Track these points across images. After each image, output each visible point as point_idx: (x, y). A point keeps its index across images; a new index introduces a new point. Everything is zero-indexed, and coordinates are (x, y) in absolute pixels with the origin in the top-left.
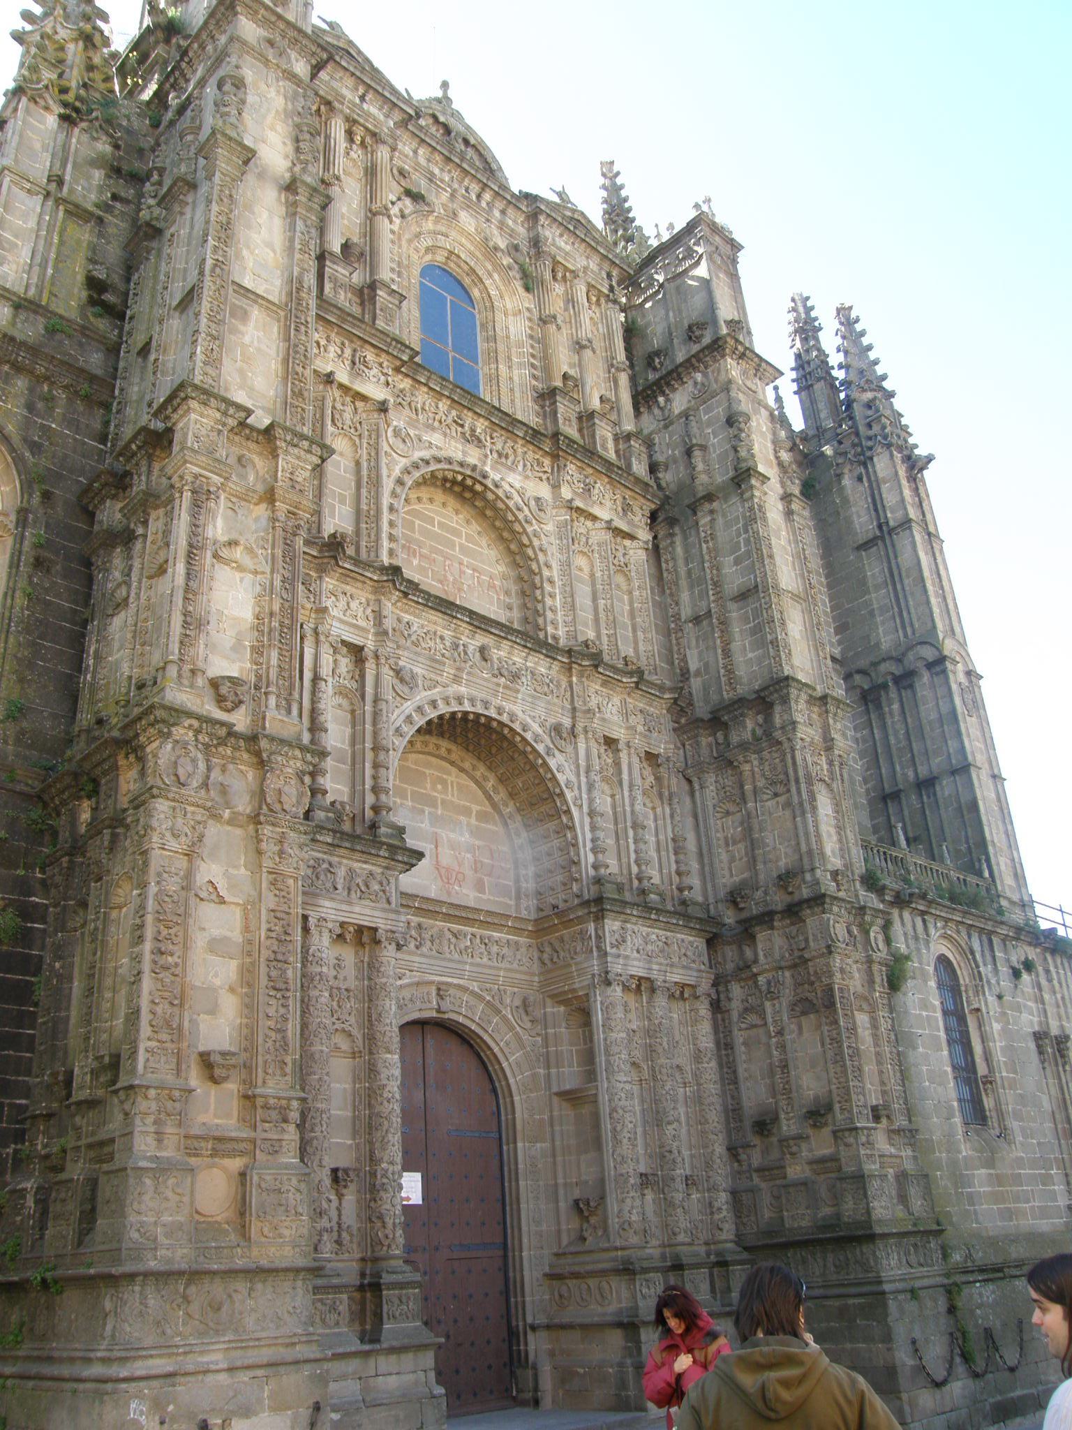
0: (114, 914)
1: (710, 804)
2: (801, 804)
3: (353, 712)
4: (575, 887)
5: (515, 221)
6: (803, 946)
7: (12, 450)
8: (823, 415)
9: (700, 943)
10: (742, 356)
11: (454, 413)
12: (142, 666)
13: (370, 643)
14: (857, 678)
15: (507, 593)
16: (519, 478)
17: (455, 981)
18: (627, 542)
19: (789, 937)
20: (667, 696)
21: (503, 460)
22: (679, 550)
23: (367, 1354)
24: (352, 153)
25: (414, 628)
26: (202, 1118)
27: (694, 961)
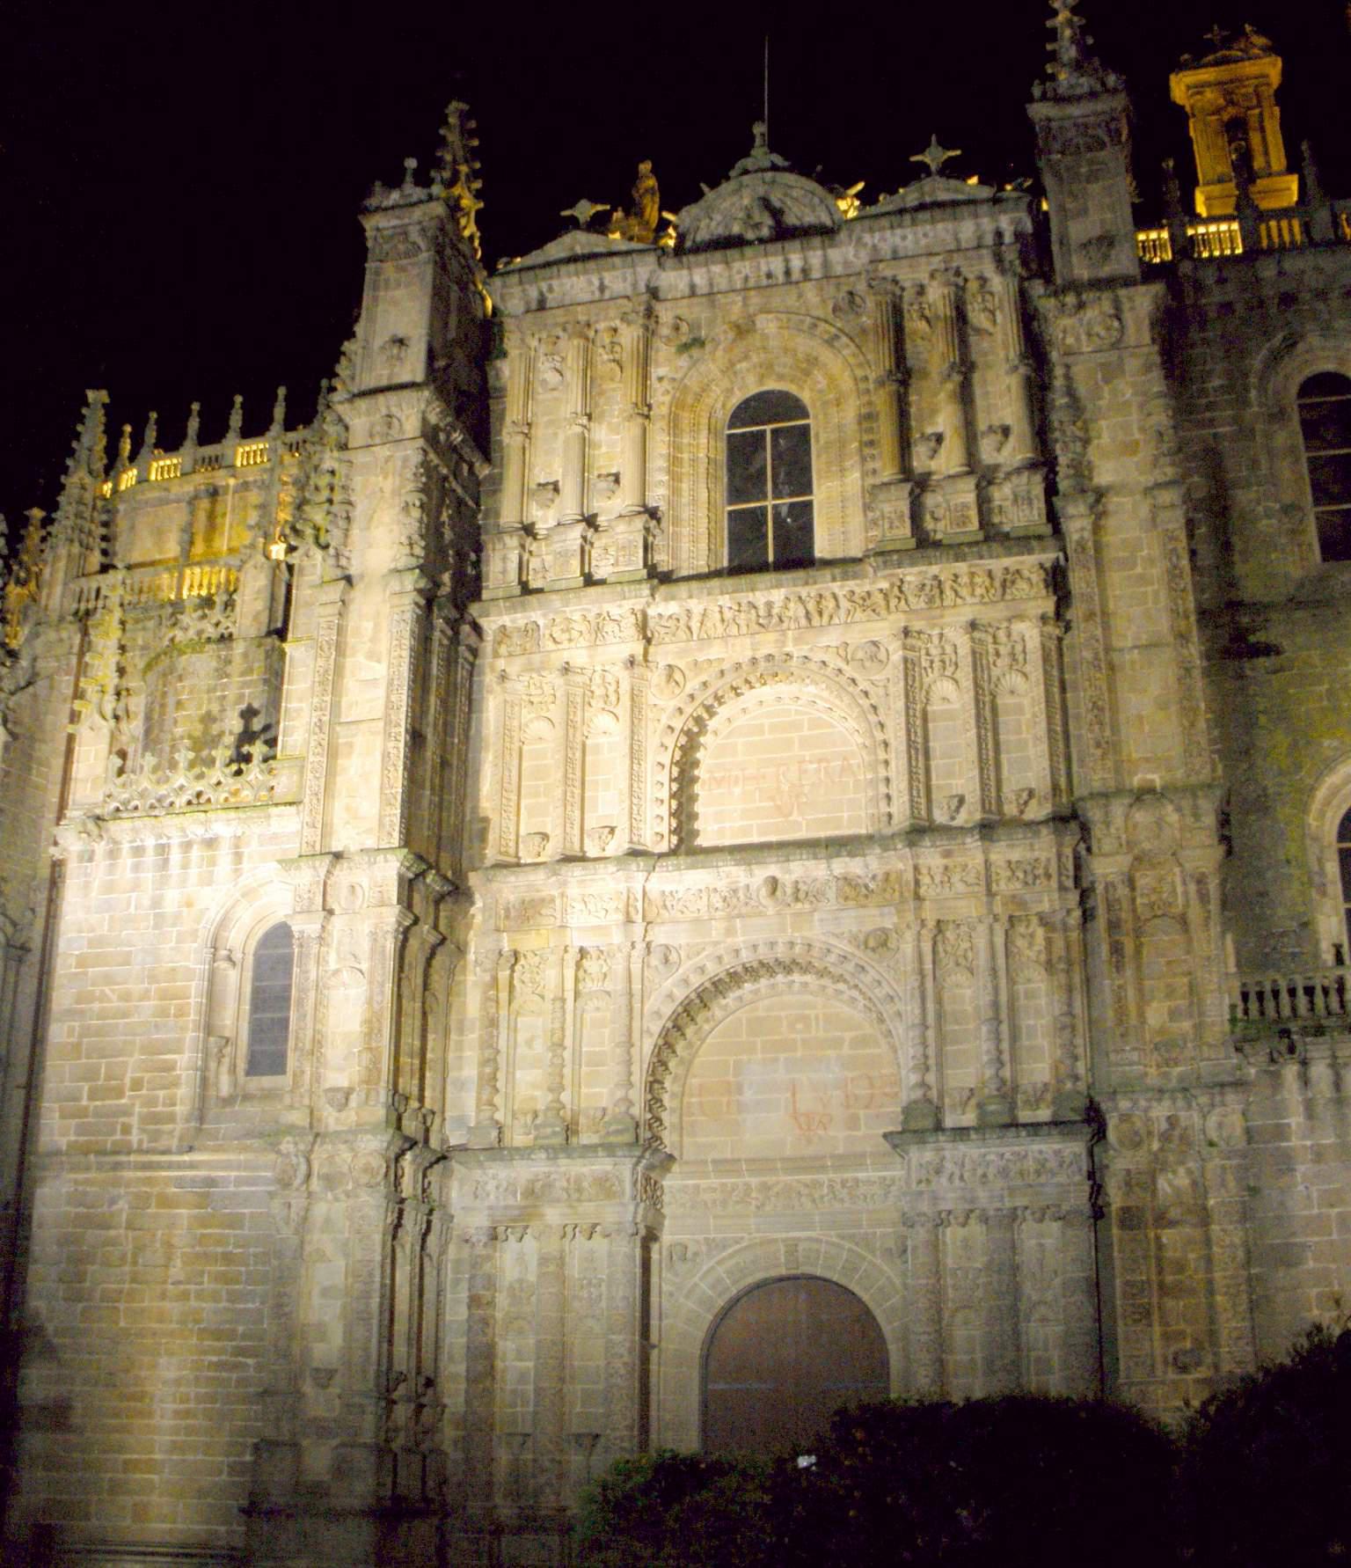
27: (1054, 1174)
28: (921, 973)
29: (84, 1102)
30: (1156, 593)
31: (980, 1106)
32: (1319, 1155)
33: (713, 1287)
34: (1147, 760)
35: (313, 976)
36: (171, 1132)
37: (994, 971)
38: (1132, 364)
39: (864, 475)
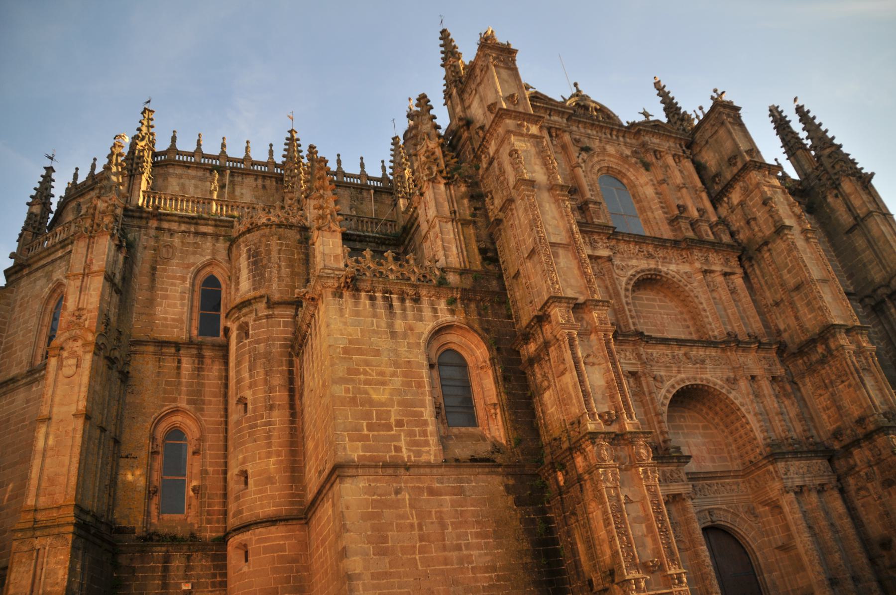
0: (591, 516)
1: (810, 393)
2: (857, 384)
3: (641, 401)
4: (758, 451)
5: (630, 139)
6: (879, 452)
7: (479, 335)
8: (806, 167)
9: (826, 463)
11: (637, 247)
12: (567, 414)
13: (639, 368)
14: (867, 300)
15: (685, 320)
16: (674, 265)
17: (715, 507)
18: (732, 277)
19: (870, 450)
20: (774, 347)
22: (758, 272)
24: (555, 142)
25: (655, 355)
29: (365, 432)
36: (428, 452)
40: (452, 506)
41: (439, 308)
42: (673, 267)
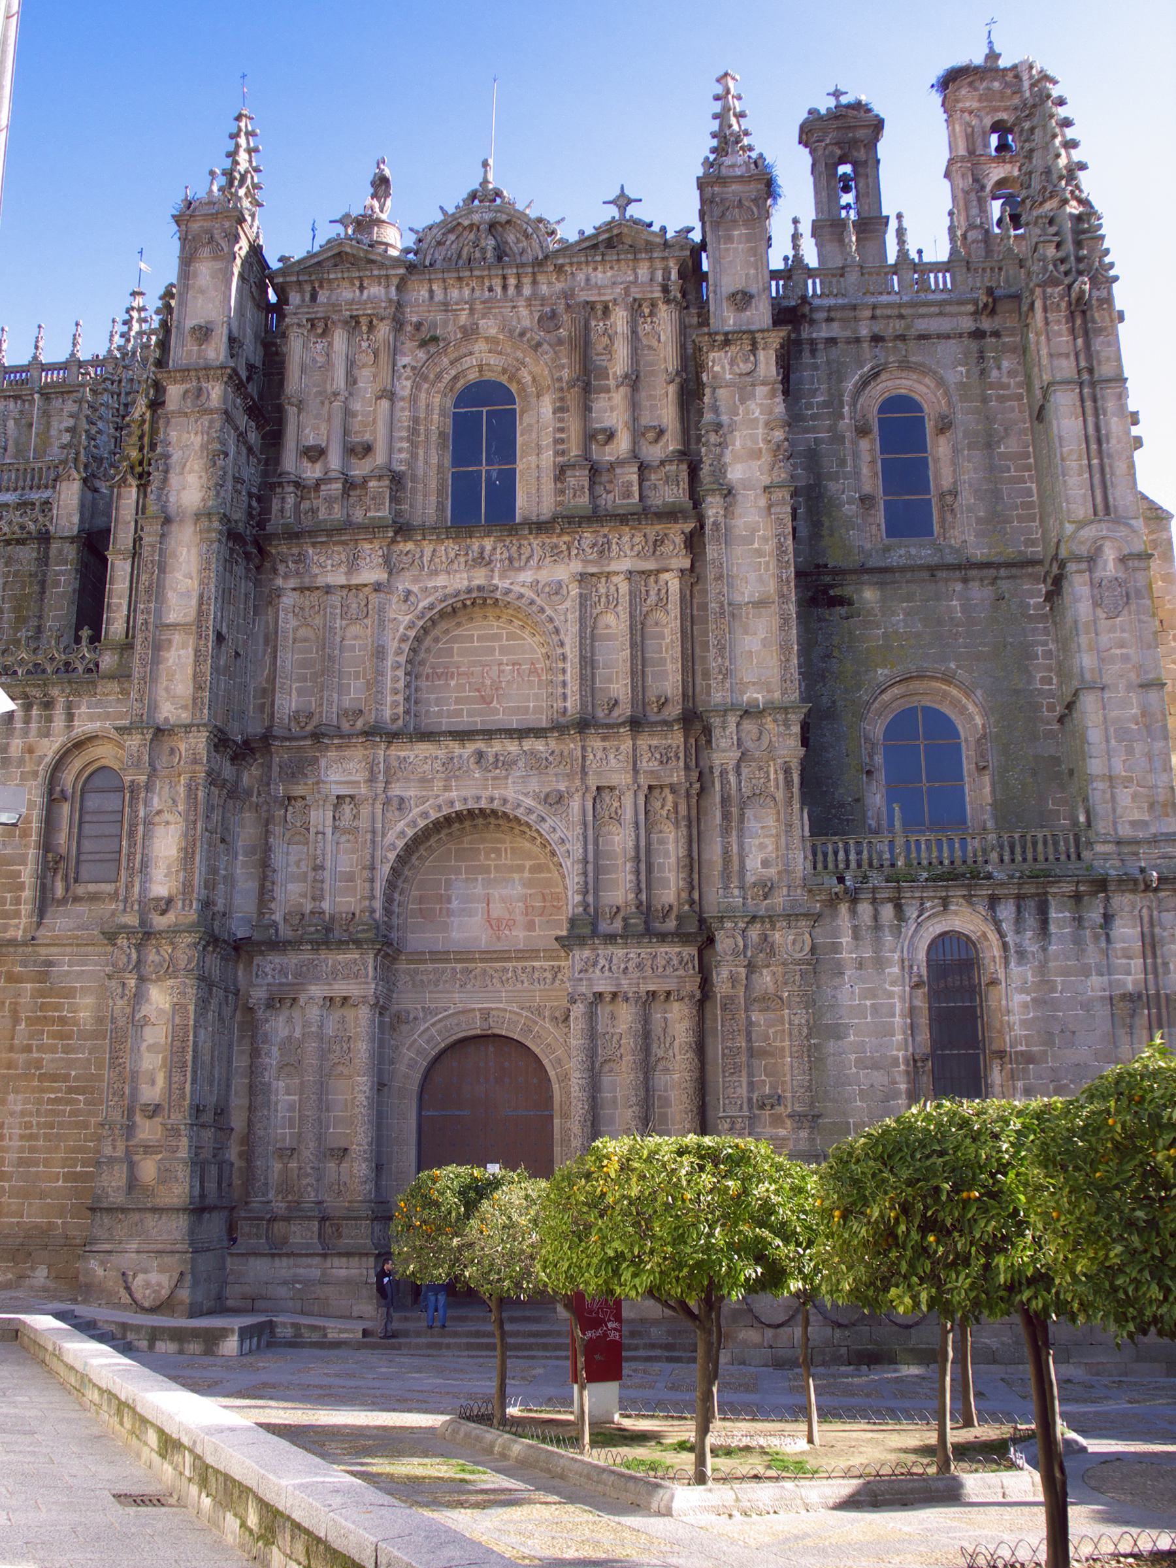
10: (727, 342)
21: (516, 565)
23: (325, 1256)
26: (141, 1136)
28: (585, 824)
30: (767, 563)
31: (625, 919)
32: (860, 965)
33: (428, 1042)
34: (754, 684)
35: (142, 814)
36: (17, 926)
37: (637, 824)
38: (761, 391)
39: (557, 453)
40: (33, 997)
41: (77, 712)
42: (527, 576)
